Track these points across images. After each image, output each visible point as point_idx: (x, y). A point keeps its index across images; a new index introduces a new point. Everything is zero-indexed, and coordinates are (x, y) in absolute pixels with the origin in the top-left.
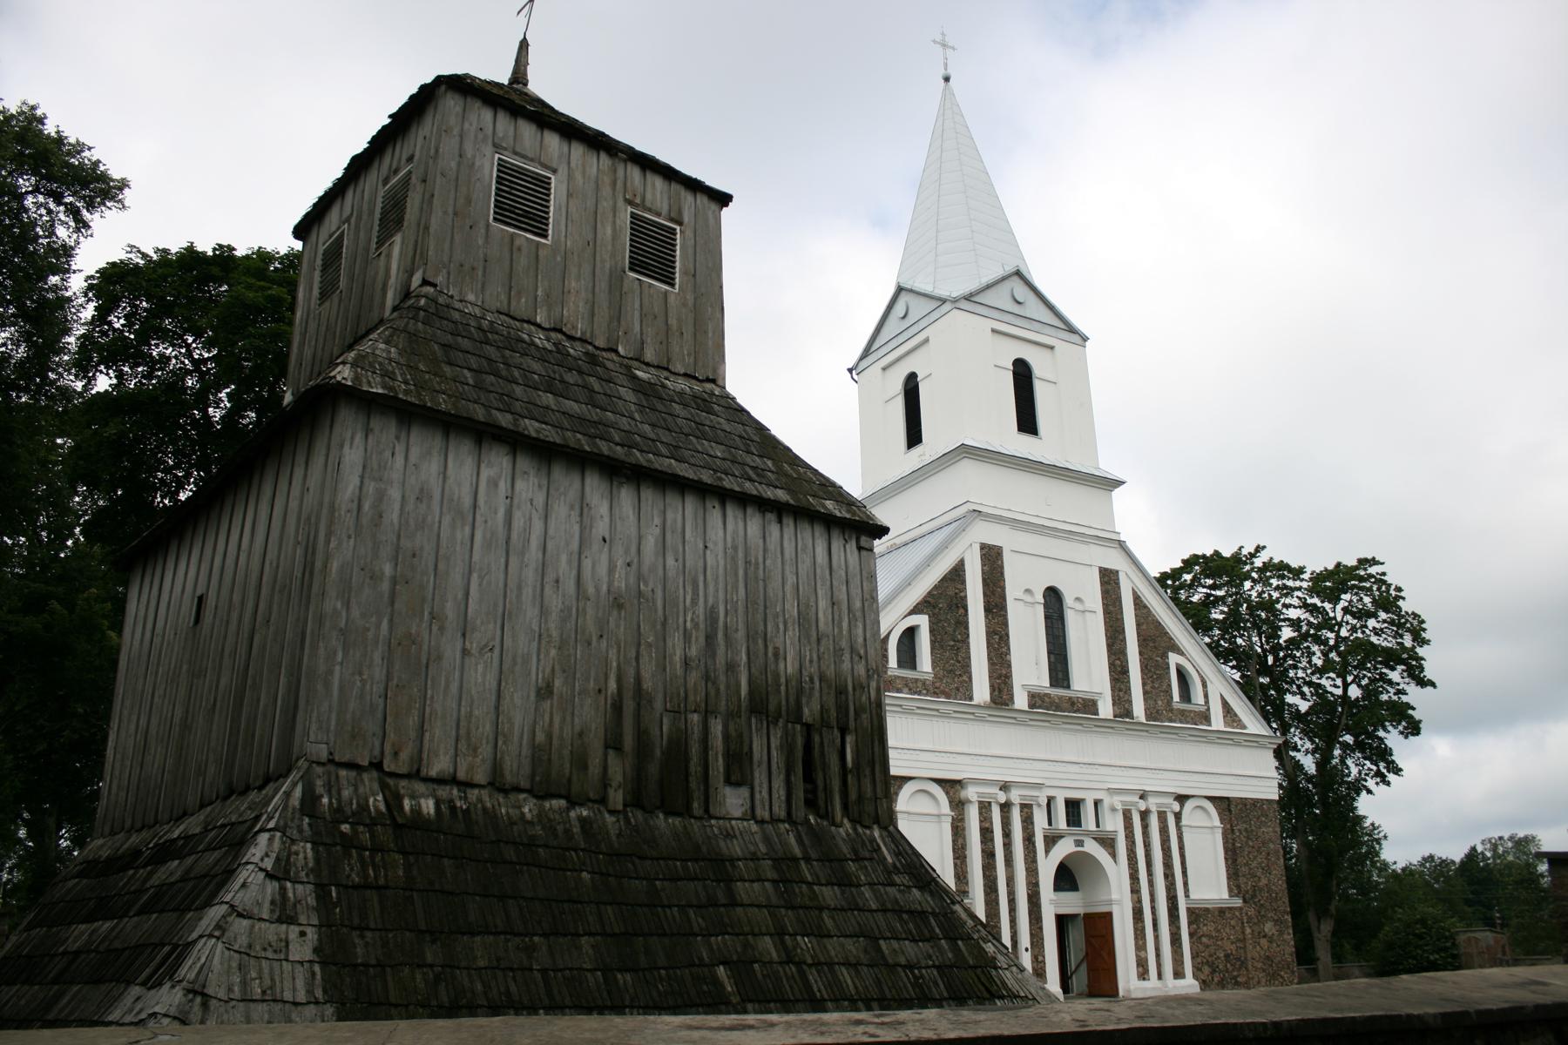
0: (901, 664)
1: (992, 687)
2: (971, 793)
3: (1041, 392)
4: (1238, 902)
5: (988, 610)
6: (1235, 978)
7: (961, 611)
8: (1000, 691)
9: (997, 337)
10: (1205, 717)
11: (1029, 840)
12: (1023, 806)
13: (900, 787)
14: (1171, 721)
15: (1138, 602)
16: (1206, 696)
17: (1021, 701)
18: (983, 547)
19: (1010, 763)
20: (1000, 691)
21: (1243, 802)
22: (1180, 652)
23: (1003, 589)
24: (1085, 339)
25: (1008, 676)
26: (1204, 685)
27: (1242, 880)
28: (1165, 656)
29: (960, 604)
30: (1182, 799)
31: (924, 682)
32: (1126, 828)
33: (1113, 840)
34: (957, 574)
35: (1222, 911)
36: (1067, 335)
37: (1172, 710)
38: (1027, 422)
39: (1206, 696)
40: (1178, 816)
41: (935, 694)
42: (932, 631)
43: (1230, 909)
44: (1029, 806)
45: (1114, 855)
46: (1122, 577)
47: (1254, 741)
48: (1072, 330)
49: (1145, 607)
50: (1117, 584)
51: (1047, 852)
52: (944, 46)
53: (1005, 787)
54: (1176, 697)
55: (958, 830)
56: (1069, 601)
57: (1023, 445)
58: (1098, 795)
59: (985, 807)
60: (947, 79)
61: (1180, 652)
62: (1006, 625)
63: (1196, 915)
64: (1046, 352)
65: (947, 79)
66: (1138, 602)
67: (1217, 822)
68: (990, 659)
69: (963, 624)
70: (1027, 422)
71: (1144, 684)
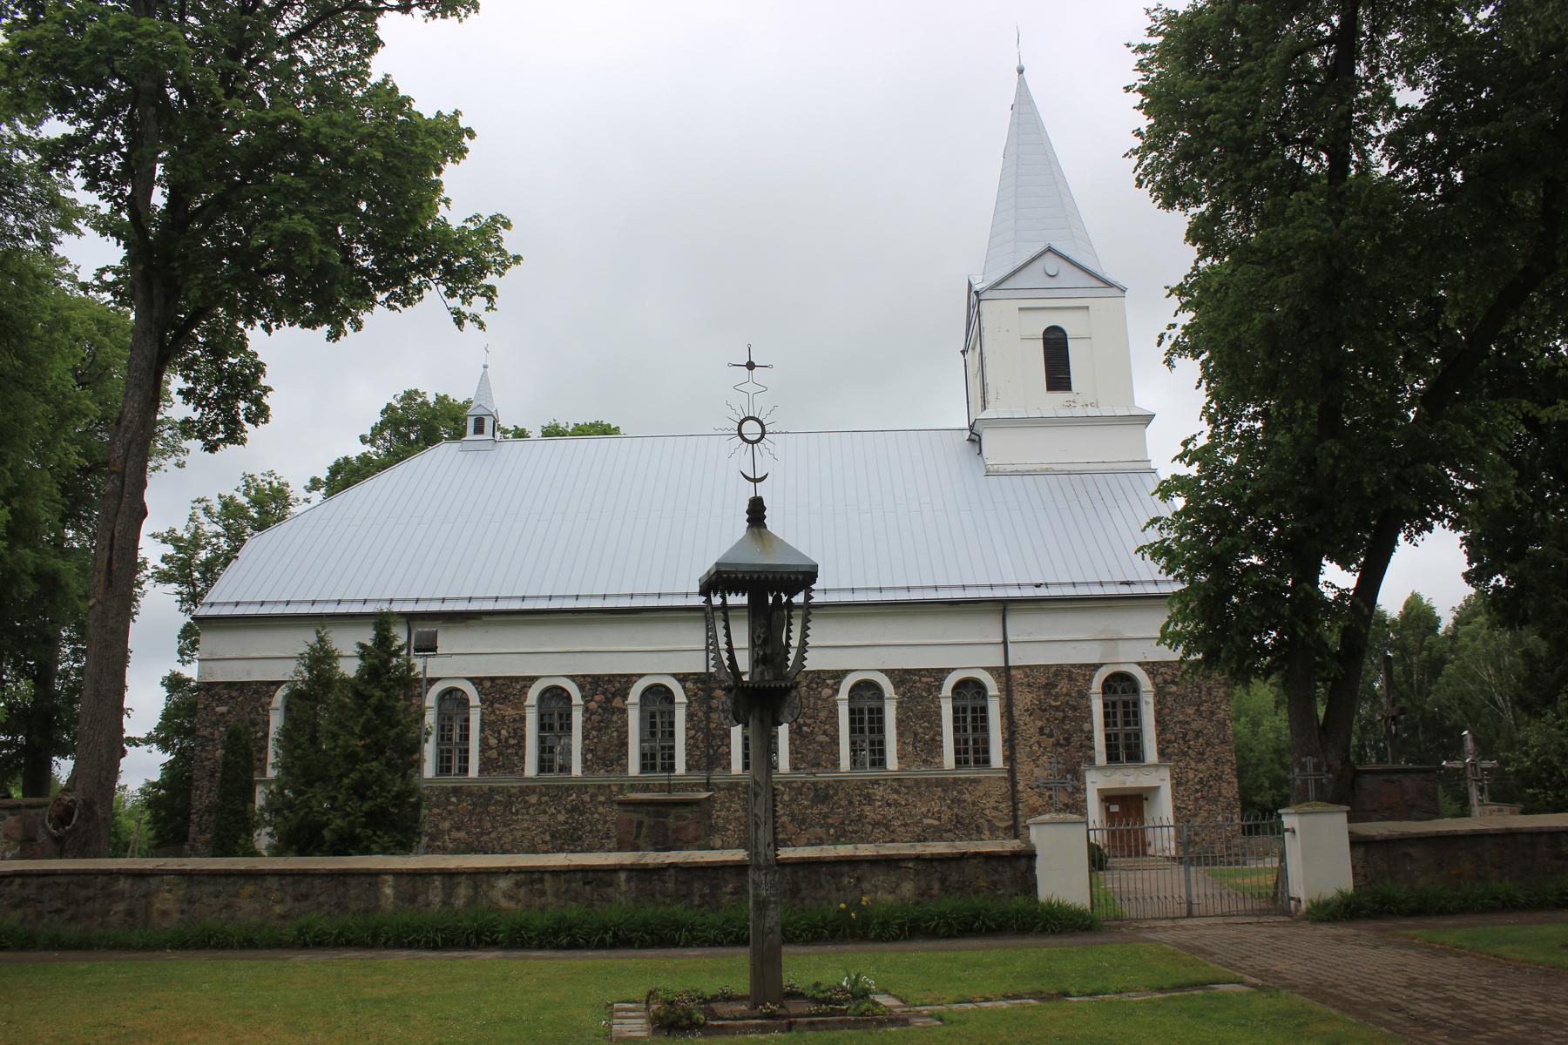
9: (1026, 315)
24: (1123, 290)
38: (1058, 376)
48: (1109, 284)
57: (1056, 403)
60: (1021, 71)
64: (1084, 312)
65: (1021, 71)
70: (1058, 376)
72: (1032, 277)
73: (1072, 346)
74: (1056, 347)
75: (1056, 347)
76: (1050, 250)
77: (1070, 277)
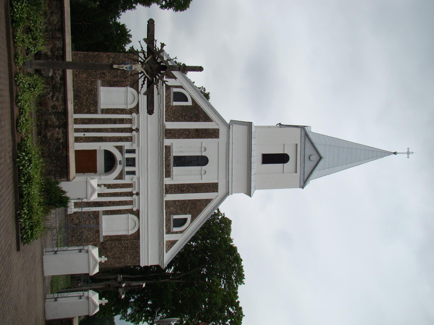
0: (175, 93)
1: (170, 130)
2: (134, 115)
3: (279, 166)
4: (102, 240)
5: (197, 130)
6: (74, 236)
7: (195, 119)
8: (170, 133)
9: (295, 146)
10: (169, 232)
11: (120, 139)
12: (131, 137)
13: (135, 89)
14: (166, 213)
15: (208, 201)
16: (177, 233)
17: (167, 142)
18: (218, 130)
19: (146, 133)
20: (170, 133)
21: (138, 247)
22: (192, 220)
23: (205, 138)
24: (303, 187)
25: (175, 137)
26: (181, 232)
27: (109, 242)
28: (190, 213)
29: (197, 119)
30: (137, 213)
31: (170, 102)
32: (126, 184)
33: (122, 179)
34: (207, 119)
35: (98, 231)
36: (302, 179)
37: (170, 214)
38: (268, 159)
39: (177, 233)
40: (131, 212)
41: (166, 106)
42: (187, 106)
43: (99, 236)
44: (131, 141)
45: (116, 179)
46: (215, 194)
47: (161, 256)
49: (207, 205)
50: (213, 191)
51: (117, 147)
52: (408, 153)
53: (137, 130)
54: (175, 217)
55: (122, 111)
56: (204, 167)
57: (257, 158)
58: (137, 173)
59: (130, 121)
60: (395, 153)
61: (192, 220)
62: (193, 137)
63: (96, 215)
64: (294, 170)
65: (395, 153)
66: (208, 201)
67: (131, 233)
68: (180, 129)
69: (190, 119)
70: (268, 159)
71: (178, 201)
72: (309, 150)
73: (280, 165)
74: (282, 158)
75: (282, 158)
76: (321, 158)
77: (309, 165)
